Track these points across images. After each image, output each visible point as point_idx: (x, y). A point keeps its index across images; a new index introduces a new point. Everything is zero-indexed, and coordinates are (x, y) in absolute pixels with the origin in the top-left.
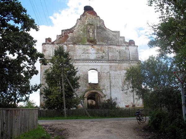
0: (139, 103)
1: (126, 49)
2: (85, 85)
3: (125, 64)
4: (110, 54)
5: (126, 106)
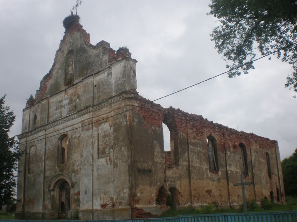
1: (108, 75)
3: (105, 109)
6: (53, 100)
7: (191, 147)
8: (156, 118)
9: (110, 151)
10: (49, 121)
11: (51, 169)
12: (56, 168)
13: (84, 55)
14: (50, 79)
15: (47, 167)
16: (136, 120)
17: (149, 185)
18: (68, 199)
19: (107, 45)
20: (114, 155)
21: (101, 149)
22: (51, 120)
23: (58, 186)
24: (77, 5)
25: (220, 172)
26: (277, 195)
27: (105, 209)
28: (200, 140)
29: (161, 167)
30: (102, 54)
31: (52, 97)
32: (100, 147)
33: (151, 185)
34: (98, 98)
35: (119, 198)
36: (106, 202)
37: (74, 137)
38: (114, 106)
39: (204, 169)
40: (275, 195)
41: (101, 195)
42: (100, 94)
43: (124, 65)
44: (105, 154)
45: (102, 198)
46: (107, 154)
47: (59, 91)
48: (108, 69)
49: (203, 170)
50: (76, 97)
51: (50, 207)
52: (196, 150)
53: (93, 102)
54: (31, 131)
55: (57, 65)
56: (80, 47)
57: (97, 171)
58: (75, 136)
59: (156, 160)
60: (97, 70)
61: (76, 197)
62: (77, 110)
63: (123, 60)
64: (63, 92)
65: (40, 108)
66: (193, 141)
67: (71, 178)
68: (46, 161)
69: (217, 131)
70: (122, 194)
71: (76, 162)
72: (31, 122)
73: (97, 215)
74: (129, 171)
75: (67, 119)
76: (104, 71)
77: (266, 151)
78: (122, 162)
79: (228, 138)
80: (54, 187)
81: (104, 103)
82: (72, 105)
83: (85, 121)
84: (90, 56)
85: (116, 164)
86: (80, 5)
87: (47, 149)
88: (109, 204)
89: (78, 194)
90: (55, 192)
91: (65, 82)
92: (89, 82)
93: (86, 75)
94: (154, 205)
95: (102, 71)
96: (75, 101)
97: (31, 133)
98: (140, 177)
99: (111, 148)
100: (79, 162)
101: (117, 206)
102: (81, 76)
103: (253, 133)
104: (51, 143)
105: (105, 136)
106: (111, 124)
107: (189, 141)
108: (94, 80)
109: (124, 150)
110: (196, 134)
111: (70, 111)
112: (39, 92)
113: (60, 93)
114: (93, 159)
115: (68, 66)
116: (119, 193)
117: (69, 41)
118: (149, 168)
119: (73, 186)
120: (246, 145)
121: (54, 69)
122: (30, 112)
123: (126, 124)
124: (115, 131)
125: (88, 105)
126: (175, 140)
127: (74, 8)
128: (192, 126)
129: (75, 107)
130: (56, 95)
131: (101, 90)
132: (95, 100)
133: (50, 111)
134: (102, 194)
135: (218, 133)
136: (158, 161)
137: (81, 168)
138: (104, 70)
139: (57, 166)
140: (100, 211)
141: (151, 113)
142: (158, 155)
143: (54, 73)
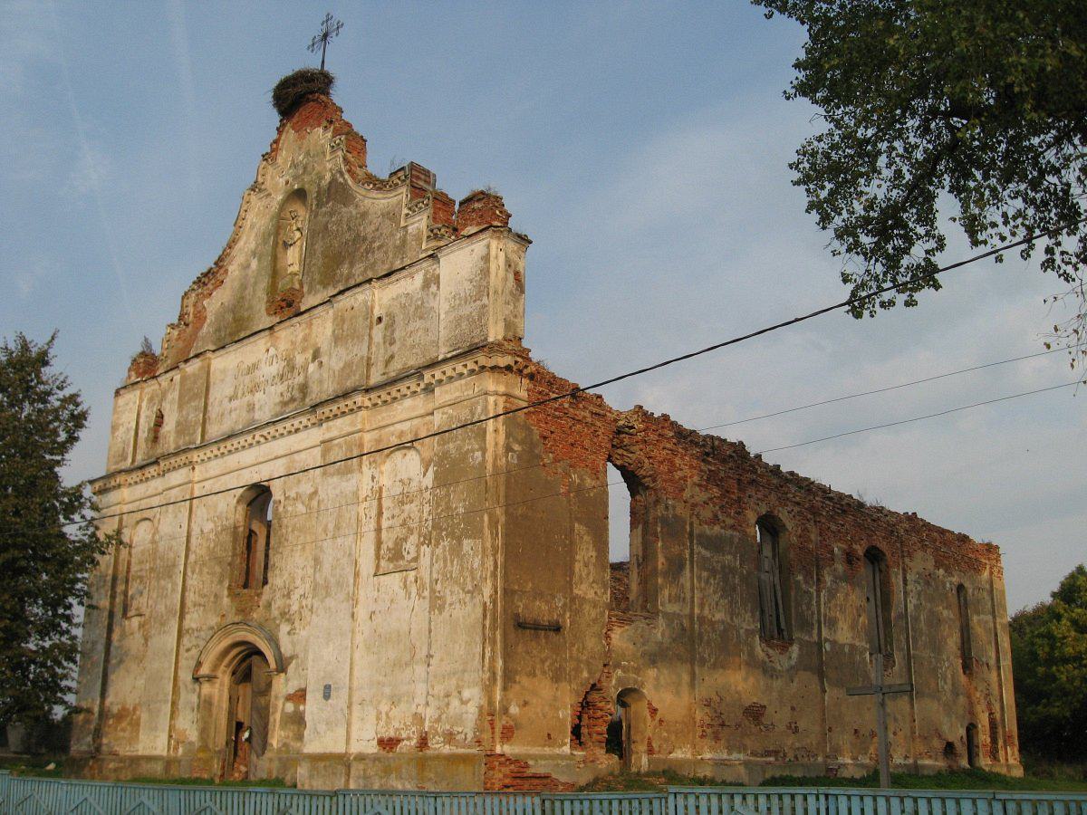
0: (459, 719)
1: (426, 285)
2: (216, 596)
3: (408, 402)
4: (335, 360)
5: (381, 742)
6: (225, 364)
7: (703, 551)
8: (587, 443)
9: (418, 552)
10: (206, 437)
11: (204, 606)
12: (226, 601)
13: (344, 210)
14: (218, 290)
15: (191, 597)
16: (516, 447)
17: (552, 679)
18: (263, 714)
19: (425, 181)
20: (432, 565)
21: (388, 539)
22: (214, 431)
23: (228, 666)
24: (325, 36)
25: (795, 649)
26: (989, 740)
27: (391, 755)
28: (732, 527)
29: (593, 615)
30: (405, 211)
31: (222, 352)
32: (384, 535)
33: (557, 678)
34: (387, 363)
35: (444, 717)
36: (397, 729)
37: (293, 495)
38: (443, 395)
39: (742, 631)
40: (983, 737)
41: (379, 702)
42: (395, 348)
43: (484, 252)
44: (401, 562)
45: (384, 716)
46: (409, 562)
47: (248, 333)
48: (425, 265)
49: (738, 636)
50: (309, 355)
51: (193, 735)
52: (720, 565)
53: (368, 377)
54: (142, 468)
55: (244, 238)
56: (330, 183)
57: (371, 617)
58: (297, 493)
59: (580, 593)
60: (387, 266)
61: (290, 707)
62: (307, 400)
63: (482, 236)
64: (262, 334)
65: (178, 387)
66: (707, 529)
67: (274, 641)
68: (189, 574)
69: (794, 499)
70: (455, 703)
71: (298, 582)
72: (143, 435)
73: (362, 772)
74: (484, 626)
75: (271, 429)
76: (413, 269)
77: (955, 579)
78: (461, 591)
79: (829, 528)
80: (215, 667)
81: (407, 383)
82: (290, 382)
83: (336, 442)
84: (364, 215)
85: (439, 598)
86: (337, 35)
87: (196, 530)
88: (409, 739)
89: (300, 696)
90: (217, 685)
91: (271, 302)
92: (355, 305)
93: (347, 280)
94: (566, 749)
95: (403, 268)
96: (305, 368)
97: (139, 473)
98: (520, 649)
99: (422, 539)
100: (308, 585)
101: (437, 746)
102: (329, 284)
103: (915, 514)
104: (208, 513)
105: (403, 499)
106: (427, 454)
107: (696, 532)
108: (373, 301)
109: (471, 552)
110: (722, 507)
111: (285, 404)
112: (176, 333)
113: (252, 339)
114: (357, 575)
115: (286, 246)
116: (446, 700)
117: (293, 161)
118: (555, 618)
119: (282, 668)
120: (888, 555)
121: (234, 253)
122: (141, 399)
123: (480, 459)
124: (442, 481)
125: (349, 384)
126: (646, 523)
127: (313, 45)
128: (708, 479)
129: (304, 389)
130: (238, 345)
131: (397, 335)
132: (373, 370)
133: (211, 399)
134: (384, 701)
135: (797, 509)
136: (586, 594)
137: (315, 606)
138: (410, 265)
139: (228, 597)
140: (375, 759)
141: (570, 424)
142: (588, 574)
143: (234, 269)
